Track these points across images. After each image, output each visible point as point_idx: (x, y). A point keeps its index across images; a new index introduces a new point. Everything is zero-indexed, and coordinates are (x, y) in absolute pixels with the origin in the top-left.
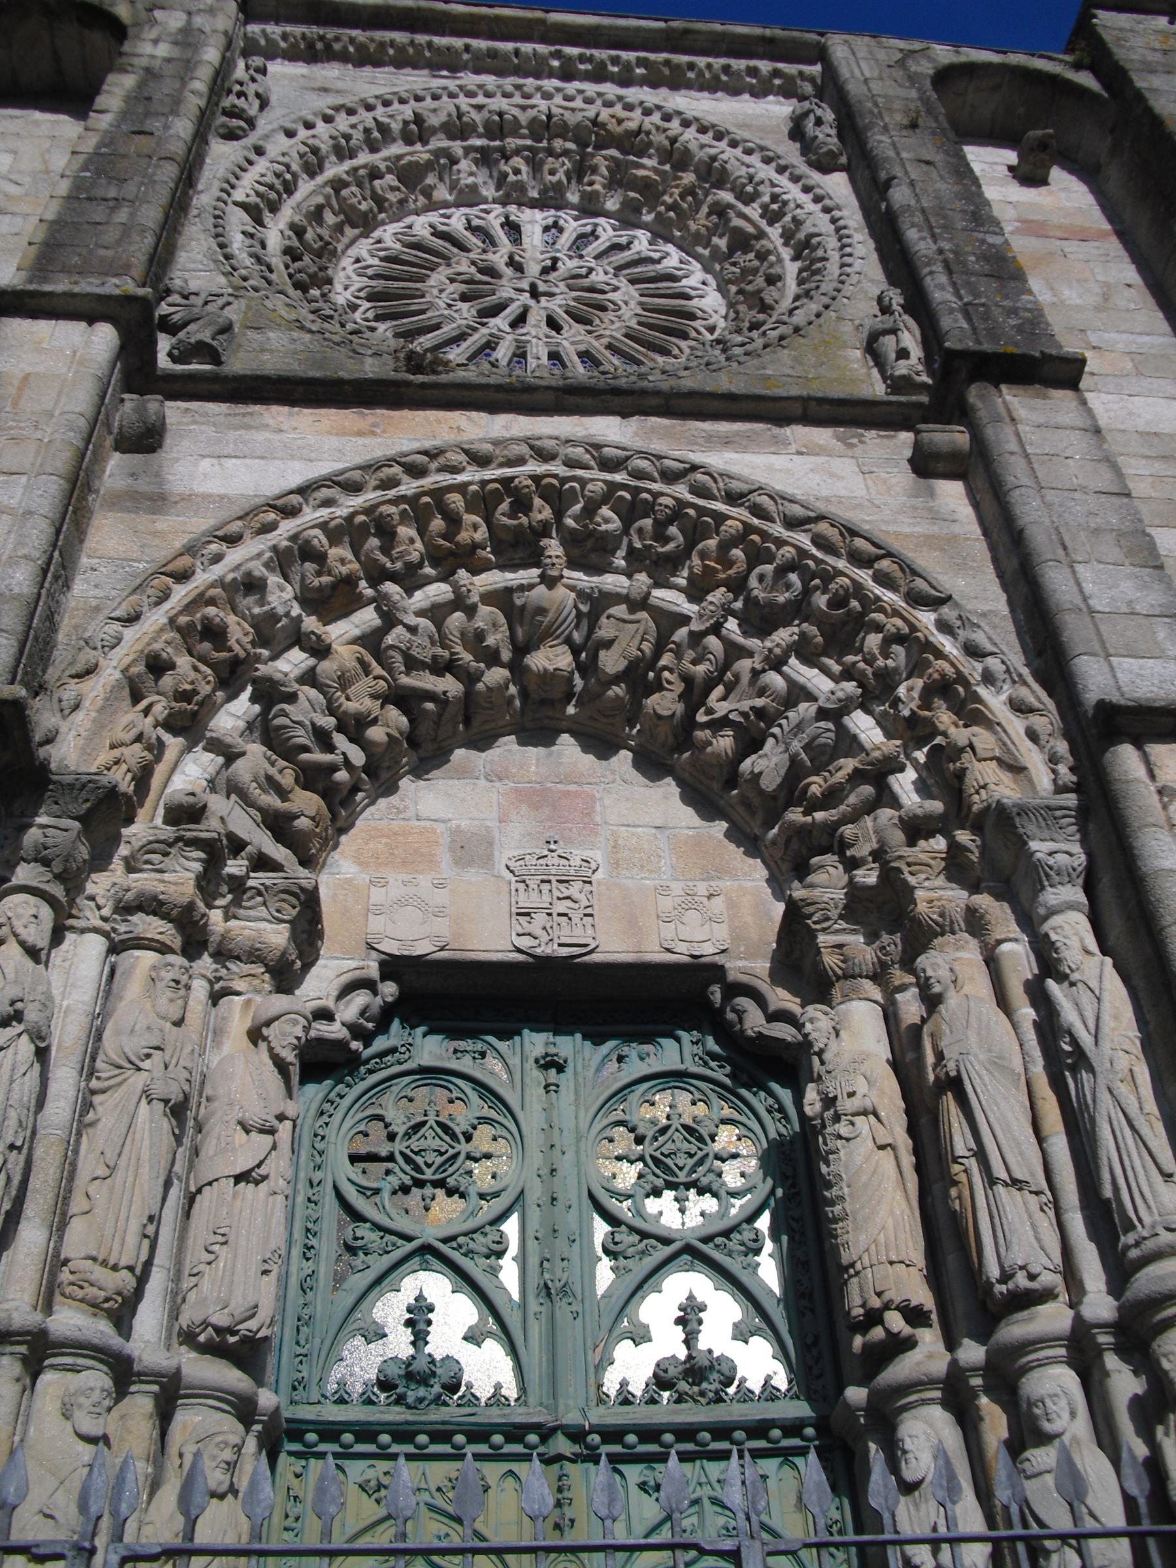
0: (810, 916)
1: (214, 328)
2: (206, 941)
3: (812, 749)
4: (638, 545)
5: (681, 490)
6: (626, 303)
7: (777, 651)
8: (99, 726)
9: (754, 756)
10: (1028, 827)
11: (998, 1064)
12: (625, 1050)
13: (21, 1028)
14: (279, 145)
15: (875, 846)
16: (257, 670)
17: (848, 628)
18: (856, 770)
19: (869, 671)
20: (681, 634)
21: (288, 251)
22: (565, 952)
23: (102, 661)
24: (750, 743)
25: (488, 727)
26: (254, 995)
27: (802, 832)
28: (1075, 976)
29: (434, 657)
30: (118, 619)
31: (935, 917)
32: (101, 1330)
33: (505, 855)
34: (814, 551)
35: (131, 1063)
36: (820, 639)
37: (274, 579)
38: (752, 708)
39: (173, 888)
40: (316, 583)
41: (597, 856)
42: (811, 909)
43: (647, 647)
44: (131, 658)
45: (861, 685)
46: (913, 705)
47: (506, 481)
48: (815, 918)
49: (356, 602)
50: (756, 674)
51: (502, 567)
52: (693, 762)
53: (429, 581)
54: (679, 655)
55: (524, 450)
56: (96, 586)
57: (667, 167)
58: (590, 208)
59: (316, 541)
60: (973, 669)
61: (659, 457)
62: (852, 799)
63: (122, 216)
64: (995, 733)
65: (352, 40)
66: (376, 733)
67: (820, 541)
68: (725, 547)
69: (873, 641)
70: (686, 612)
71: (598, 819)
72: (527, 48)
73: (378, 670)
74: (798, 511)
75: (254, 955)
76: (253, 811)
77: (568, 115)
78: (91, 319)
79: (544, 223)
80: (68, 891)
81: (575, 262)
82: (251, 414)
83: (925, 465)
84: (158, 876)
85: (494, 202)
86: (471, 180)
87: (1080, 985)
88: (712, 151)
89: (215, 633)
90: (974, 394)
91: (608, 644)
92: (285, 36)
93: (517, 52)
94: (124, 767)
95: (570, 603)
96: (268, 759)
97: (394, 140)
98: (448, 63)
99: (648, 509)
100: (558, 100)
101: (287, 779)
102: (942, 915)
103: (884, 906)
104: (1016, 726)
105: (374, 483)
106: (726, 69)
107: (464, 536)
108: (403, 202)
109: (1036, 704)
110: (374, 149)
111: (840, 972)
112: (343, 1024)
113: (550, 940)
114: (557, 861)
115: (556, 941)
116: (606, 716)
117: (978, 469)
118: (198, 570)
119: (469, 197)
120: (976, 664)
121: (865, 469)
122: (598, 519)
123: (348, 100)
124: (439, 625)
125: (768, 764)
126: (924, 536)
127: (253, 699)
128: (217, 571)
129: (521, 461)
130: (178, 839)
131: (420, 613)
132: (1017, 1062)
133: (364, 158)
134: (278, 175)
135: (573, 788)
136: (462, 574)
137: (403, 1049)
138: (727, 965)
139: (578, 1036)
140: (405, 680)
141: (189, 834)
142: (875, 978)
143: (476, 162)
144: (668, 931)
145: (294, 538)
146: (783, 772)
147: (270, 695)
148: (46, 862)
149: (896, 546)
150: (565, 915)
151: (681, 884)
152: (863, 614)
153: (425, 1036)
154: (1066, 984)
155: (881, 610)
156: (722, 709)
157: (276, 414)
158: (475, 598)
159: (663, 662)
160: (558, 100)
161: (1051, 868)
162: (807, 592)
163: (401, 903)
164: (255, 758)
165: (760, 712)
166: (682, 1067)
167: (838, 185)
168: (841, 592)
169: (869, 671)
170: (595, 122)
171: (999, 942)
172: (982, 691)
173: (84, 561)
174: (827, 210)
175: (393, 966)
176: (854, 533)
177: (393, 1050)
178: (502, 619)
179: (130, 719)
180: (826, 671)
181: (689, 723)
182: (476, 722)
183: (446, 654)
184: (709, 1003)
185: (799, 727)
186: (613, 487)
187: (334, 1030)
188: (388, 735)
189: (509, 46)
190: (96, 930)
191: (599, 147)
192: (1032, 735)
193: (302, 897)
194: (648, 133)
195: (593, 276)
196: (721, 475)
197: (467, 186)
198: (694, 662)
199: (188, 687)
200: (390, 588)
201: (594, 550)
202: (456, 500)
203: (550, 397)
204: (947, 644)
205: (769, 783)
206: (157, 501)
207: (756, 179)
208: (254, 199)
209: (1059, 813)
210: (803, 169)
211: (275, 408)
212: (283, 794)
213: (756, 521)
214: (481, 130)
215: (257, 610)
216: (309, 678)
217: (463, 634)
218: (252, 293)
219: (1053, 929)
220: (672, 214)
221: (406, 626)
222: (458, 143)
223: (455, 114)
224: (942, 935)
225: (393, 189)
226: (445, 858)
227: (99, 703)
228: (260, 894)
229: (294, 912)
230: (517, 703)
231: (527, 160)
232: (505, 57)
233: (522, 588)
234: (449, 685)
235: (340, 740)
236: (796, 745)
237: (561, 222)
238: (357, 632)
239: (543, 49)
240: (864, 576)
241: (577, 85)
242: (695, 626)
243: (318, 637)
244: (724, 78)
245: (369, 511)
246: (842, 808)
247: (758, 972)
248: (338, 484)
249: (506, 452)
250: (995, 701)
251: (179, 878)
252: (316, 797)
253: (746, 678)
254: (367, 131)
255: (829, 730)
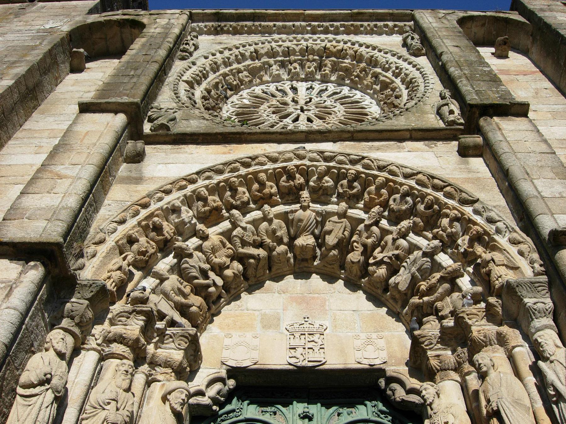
0: (423, 343)
1: (167, 119)
2: (146, 357)
3: (421, 271)
4: (341, 191)
5: (359, 167)
6: (339, 111)
7: (403, 230)
8: (103, 264)
9: (395, 276)
10: (522, 292)
11: (517, 403)
12: (341, 410)
13: (48, 386)
14: (201, 62)
15: (452, 309)
16: (175, 244)
17: (434, 218)
18: (441, 277)
19: (444, 234)
20: (361, 227)
21: (204, 98)
22: (311, 364)
23: (107, 238)
24: (394, 271)
25: (279, 271)
26: (167, 381)
27: (418, 307)
28: (552, 358)
29: (254, 240)
30: (116, 222)
31: (482, 338)
33: (284, 324)
34: (417, 187)
35: (101, 406)
36: (422, 224)
37: (184, 208)
38: (393, 255)
39: (129, 332)
40: (203, 210)
41: (326, 323)
42: (424, 339)
43: (346, 233)
44: (119, 237)
45: (441, 241)
46: (465, 247)
47: (284, 168)
48: (426, 343)
49: (221, 219)
50: (394, 240)
51: (284, 204)
52: (369, 282)
53: (253, 210)
54: (360, 235)
55: (292, 155)
56: (109, 211)
57: (355, 62)
58: (325, 80)
59: (202, 193)
60: (491, 228)
61: (349, 155)
62: (440, 290)
63: (135, 80)
64: (503, 254)
65: (231, 26)
66: (228, 272)
67: (419, 182)
68: (378, 189)
69: (445, 222)
70: (363, 218)
71: (327, 308)
73: (229, 245)
74: (408, 171)
75: (167, 364)
76: (170, 303)
77: (314, 46)
78: (116, 113)
79: (307, 87)
80: (82, 332)
81: (319, 99)
82: (181, 148)
84: (123, 327)
85: (287, 80)
86: (277, 72)
87: (555, 362)
88: (371, 54)
89: (158, 229)
90: (482, 122)
91: (330, 232)
92: (206, 26)
93: (294, 26)
94: (112, 280)
95: (313, 217)
96: (180, 282)
97: (247, 59)
98: (268, 31)
99: (345, 176)
100: (311, 41)
101: (187, 290)
102: (485, 337)
103: (458, 336)
104: (513, 250)
105: (228, 170)
106: (376, 26)
107: (267, 191)
108: (251, 81)
109: (522, 240)
110: (239, 63)
111: (439, 368)
112: (209, 397)
113: (304, 359)
114: (308, 325)
115: (307, 360)
116: (330, 265)
117: (487, 151)
118: (152, 204)
119: (277, 79)
120: (492, 226)
121: (438, 155)
122: (324, 181)
123: (228, 46)
124: (257, 228)
125: (402, 279)
126: (465, 178)
127: (174, 257)
128: (160, 204)
129: (290, 160)
130: (134, 311)
131: (248, 223)
132: (527, 402)
133: (235, 66)
134: (201, 72)
135: (316, 295)
136: (266, 207)
137: (238, 410)
138: (387, 369)
139: (319, 405)
140: (241, 250)
141: (138, 309)
142: (455, 370)
143: (279, 66)
144: (359, 355)
145: (194, 192)
146: (408, 281)
148: (72, 318)
149: (452, 181)
150: (312, 348)
151: (365, 334)
152: (440, 211)
153: (248, 405)
154: (548, 362)
155: (448, 208)
156: (380, 256)
157: (191, 148)
158: (271, 216)
159: (353, 239)
160: (311, 41)
161: (536, 310)
162: (415, 204)
163: (237, 344)
164: (173, 280)
165: (397, 257)
166: (367, 417)
167: (423, 61)
168: (430, 202)
169: (444, 234)
170: (325, 48)
171: (514, 347)
172: (496, 237)
173: (106, 202)
174: (418, 69)
175: (233, 372)
176: (433, 178)
177: (233, 411)
178: (284, 225)
179: (117, 261)
180: (426, 238)
181: (366, 264)
182: (274, 269)
183: (259, 239)
184: (379, 387)
185: (415, 261)
186: (329, 168)
187: (205, 400)
188: (234, 273)
189: (291, 23)
190: (94, 349)
191: (327, 57)
192: (521, 253)
193: (190, 338)
194: (346, 50)
195: (326, 103)
196: (375, 160)
197: (276, 75)
198: (367, 238)
199: (144, 249)
200: (235, 212)
201: (323, 195)
202: (263, 176)
203: (303, 136)
204: (477, 219)
205: (403, 287)
206: (139, 180)
207: (389, 62)
208: (190, 79)
209: (537, 285)
210: (408, 56)
211: (190, 146)
212: (185, 296)
213: (391, 177)
214: (281, 54)
215: (176, 220)
216: (199, 248)
217: (267, 232)
218: (186, 108)
219: (539, 336)
220: (357, 79)
221: (241, 227)
222: (273, 59)
223: (270, 49)
224: (486, 346)
225: (247, 77)
226: (258, 326)
227: (104, 254)
228: (171, 337)
229: (186, 345)
230: (292, 260)
231: (300, 64)
232: (289, 27)
233: (293, 212)
234: (261, 252)
235: (211, 274)
236: (414, 269)
237: (314, 86)
238: (221, 231)
239: (303, 24)
240: (440, 195)
241: (318, 36)
242: (367, 222)
243: (203, 231)
244: (375, 29)
245: (226, 181)
246: (436, 294)
247: (401, 371)
248: (213, 170)
249: (284, 157)
250: (502, 241)
251: (133, 328)
252: (200, 298)
253: (390, 242)
254: (236, 56)
255: (428, 261)
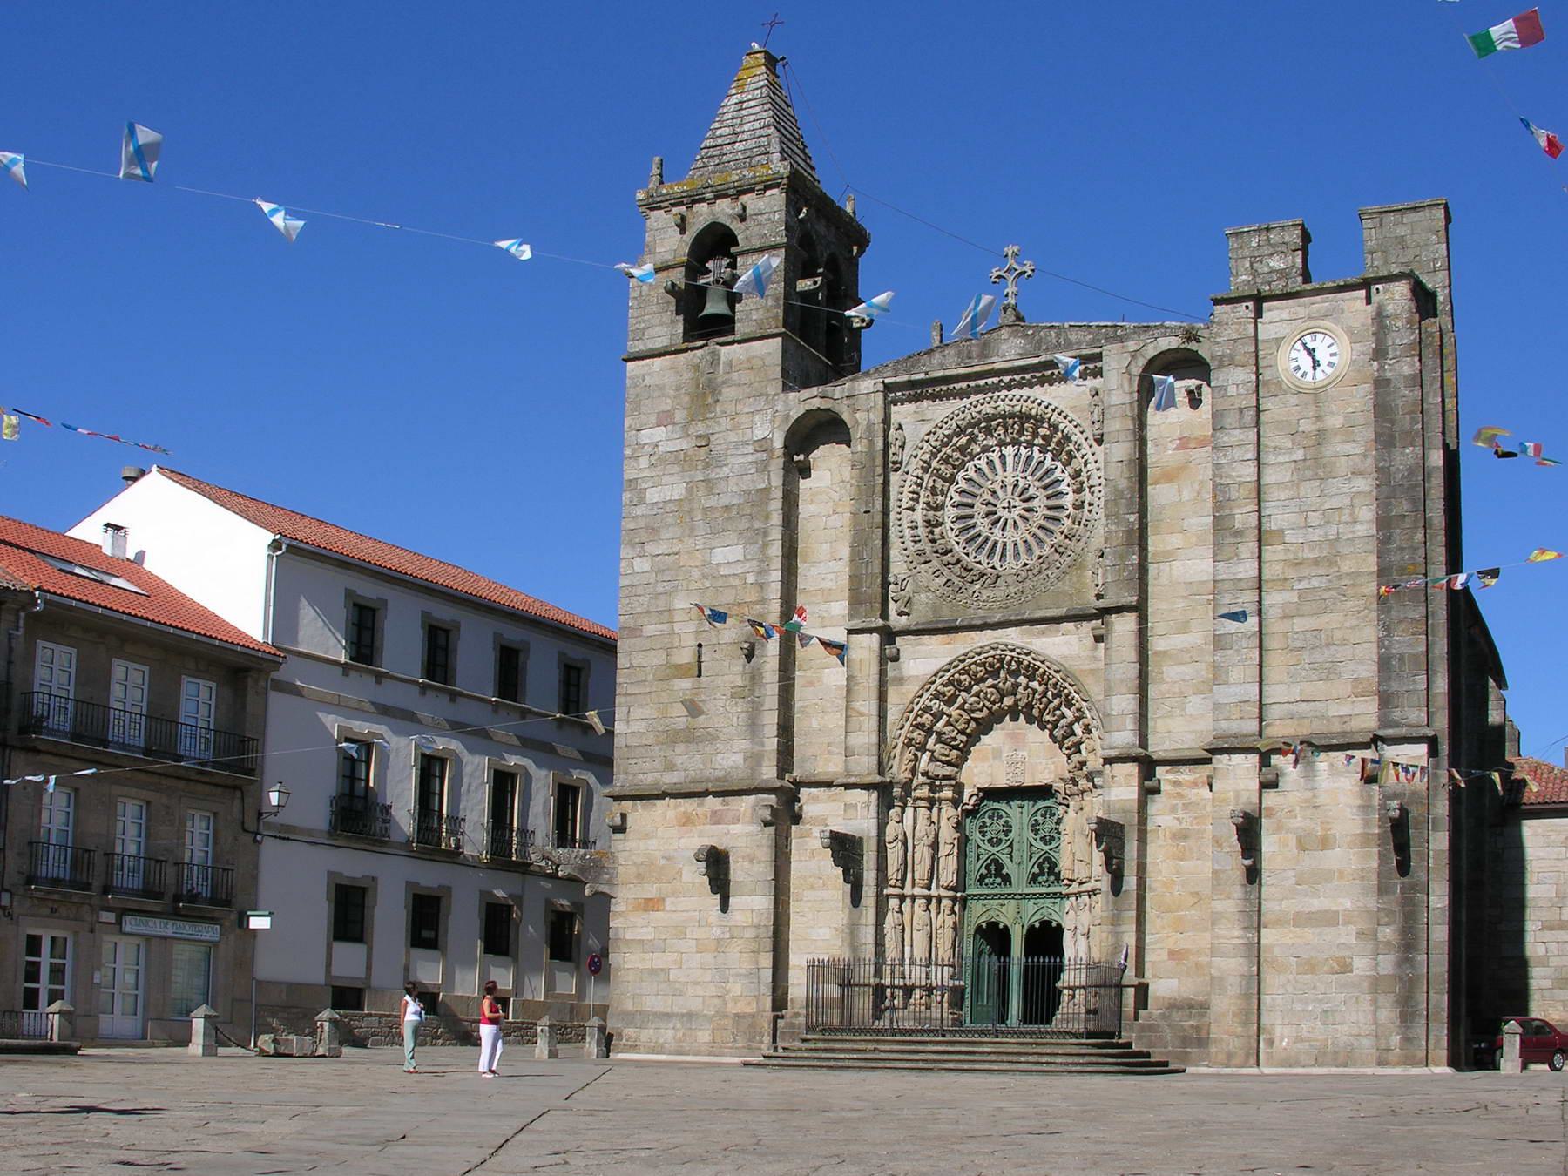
32: (926, 892)
72: (989, 381)
83: (1099, 639)
98: (962, 394)
125: (1058, 733)
147: (939, 734)
175: (980, 790)
216: (948, 723)
251: (924, 792)
